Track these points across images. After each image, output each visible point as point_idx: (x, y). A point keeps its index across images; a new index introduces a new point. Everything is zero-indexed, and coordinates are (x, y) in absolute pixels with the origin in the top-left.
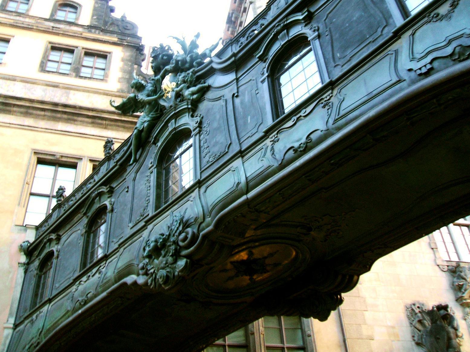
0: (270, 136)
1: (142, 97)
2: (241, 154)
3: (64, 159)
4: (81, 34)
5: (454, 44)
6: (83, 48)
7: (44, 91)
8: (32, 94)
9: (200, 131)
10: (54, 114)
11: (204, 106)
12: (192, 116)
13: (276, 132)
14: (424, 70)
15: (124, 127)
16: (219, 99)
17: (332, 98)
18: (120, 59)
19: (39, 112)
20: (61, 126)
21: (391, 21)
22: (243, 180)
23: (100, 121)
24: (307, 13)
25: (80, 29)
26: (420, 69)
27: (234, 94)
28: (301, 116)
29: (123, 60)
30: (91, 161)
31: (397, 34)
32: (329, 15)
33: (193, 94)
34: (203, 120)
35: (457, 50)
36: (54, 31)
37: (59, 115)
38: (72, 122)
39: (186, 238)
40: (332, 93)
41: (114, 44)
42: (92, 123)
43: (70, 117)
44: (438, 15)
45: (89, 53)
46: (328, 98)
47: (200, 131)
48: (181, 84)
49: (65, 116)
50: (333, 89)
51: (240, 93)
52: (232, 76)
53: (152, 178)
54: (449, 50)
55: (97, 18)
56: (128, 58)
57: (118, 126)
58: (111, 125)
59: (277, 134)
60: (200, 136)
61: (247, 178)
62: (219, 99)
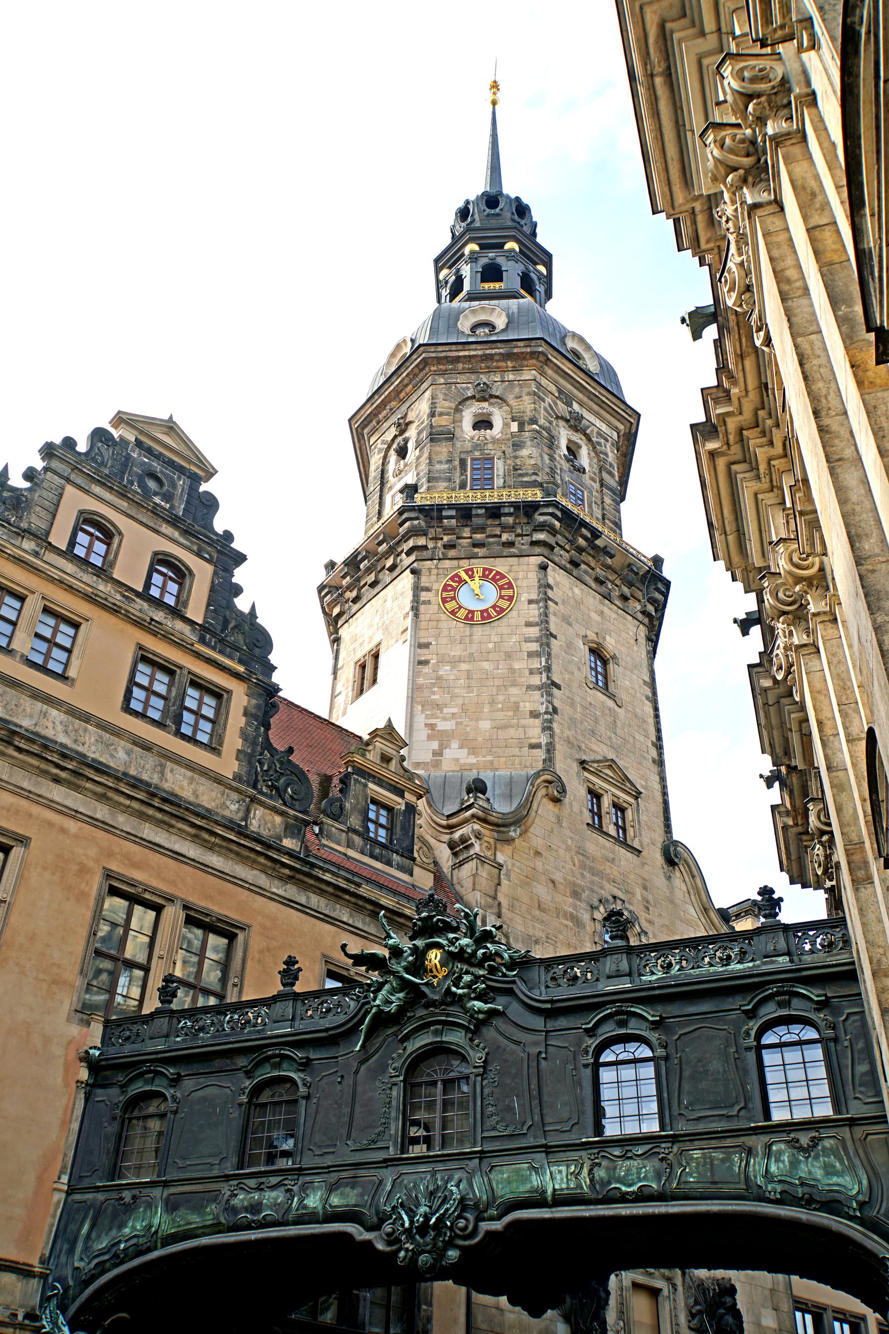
0: (589, 1151)
1: (397, 967)
2: (547, 1150)
3: (147, 896)
4: (192, 645)
5: (806, 1189)
6: (189, 673)
7: (128, 753)
8: (112, 756)
9: (484, 1073)
10: (144, 808)
11: (489, 1033)
12: (471, 1040)
13: (596, 1151)
14: (772, 1196)
15: (238, 854)
16: (518, 1043)
17: (671, 1154)
18: (242, 711)
19: (122, 800)
20: (149, 832)
21: (751, 1106)
22: (550, 1191)
23: (206, 836)
24: (658, 1018)
25: (186, 629)
26: (770, 1192)
27: (540, 1053)
28: (631, 1151)
29: (245, 714)
30: (186, 907)
31: (756, 1131)
32: (682, 1037)
33: (480, 1011)
34: (489, 1058)
35: (806, 1196)
36: (151, 627)
37: (150, 812)
38: (166, 827)
39: (465, 1228)
40: (672, 1148)
41: (236, 675)
42: (196, 836)
43: (166, 818)
44: (798, 1141)
45: (197, 683)
46: (667, 1151)
47: (484, 1073)
48: (463, 988)
49: (159, 816)
50: (673, 1143)
51: (548, 1055)
52: (538, 1022)
53: (394, 1093)
54: (800, 1191)
55: (215, 611)
56: (254, 711)
57: (231, 851)
58: (220, 846)
59: (598, 1153)
60: (482, 1080)
61: (554, 1190)
62: (518, 1043)
